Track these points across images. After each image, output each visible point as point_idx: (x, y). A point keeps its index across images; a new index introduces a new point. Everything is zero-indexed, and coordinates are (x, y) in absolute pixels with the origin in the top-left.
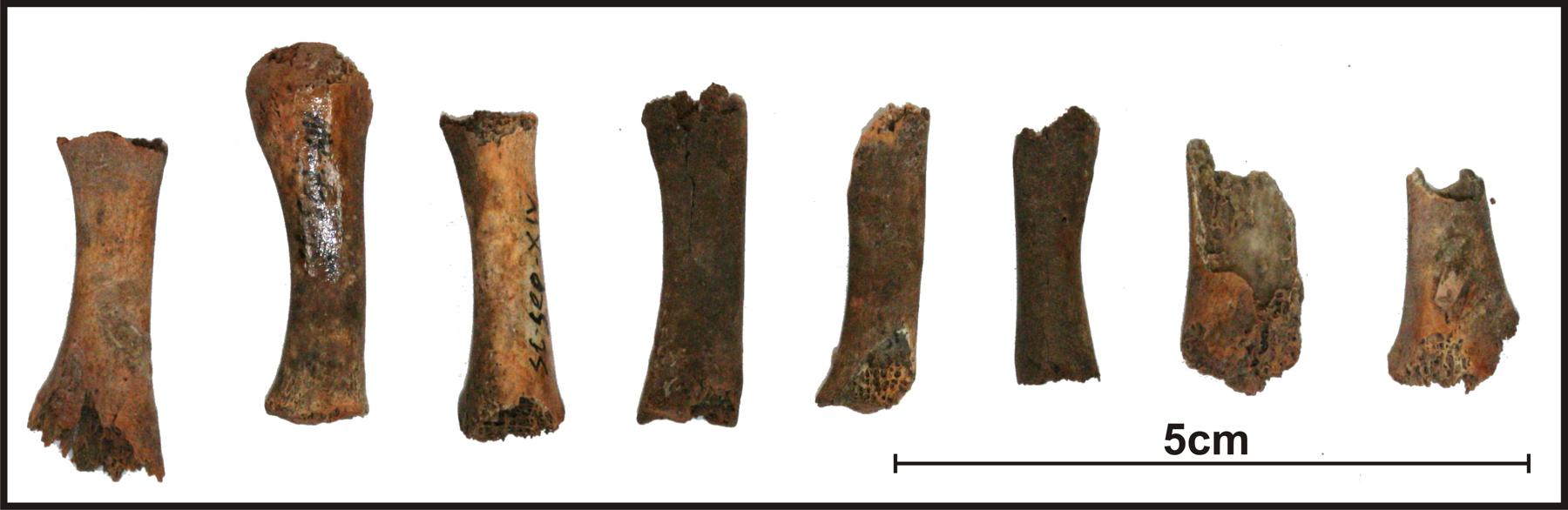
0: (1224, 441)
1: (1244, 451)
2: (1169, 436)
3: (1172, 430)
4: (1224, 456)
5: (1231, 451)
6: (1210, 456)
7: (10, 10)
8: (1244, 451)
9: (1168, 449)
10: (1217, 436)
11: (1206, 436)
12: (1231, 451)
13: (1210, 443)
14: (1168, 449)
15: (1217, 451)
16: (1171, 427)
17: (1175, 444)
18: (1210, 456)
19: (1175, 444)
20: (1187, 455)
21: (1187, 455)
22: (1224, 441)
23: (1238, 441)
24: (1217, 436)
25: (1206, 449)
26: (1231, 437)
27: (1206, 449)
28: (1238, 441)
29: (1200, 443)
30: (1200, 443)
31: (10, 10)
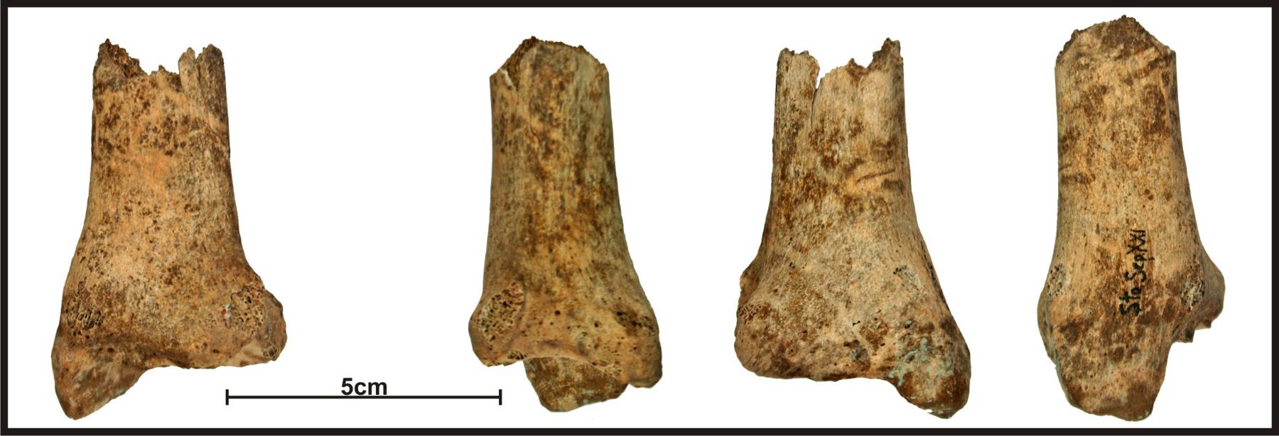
0: (374, 387)
1: (385, 392)
2: (344, 385)
3: (345, 382)
4: (374, 393)
5: (378, 392)
8: (385, 392)
10: (370, 385)
12: (378, 392)
13: (366, 388)
16: (345, 380)
17: (347, 389)
19: (347, 389)
20: (354, 393)
21: (354, 393)
22: (374, 387)
23: (381, 387)
24: (370, 385)
26: (378, 385)
28: (381, 387)
29: (361, 389)
30: (361, 389)
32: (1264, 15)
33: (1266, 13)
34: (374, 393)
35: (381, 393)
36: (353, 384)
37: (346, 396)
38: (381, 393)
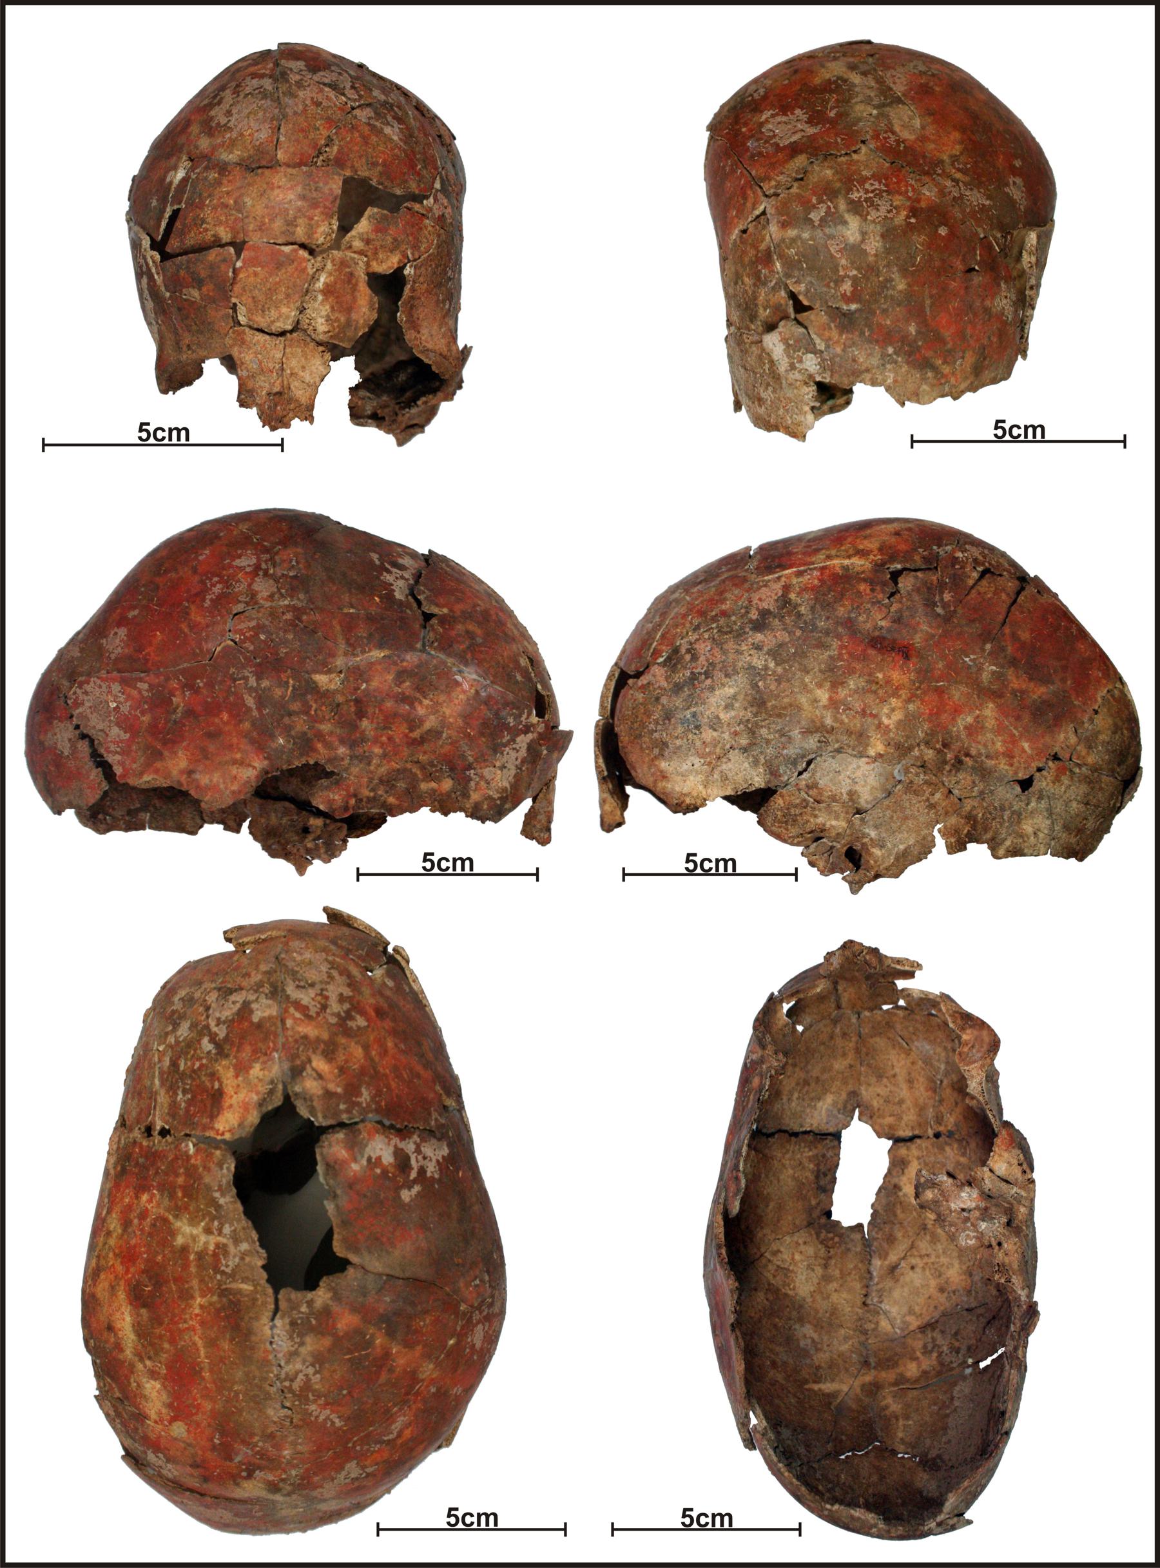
0: (175, 433)
1: (187, 439)
2: (141, 430)
4: (175, 441)
5: (179, 439)
6: (166, 441)
7: (8, 8)
8: (187, 439)
9: (140, 438)
10: (171, 430)
11: (163, 430)
12: (179, 439)
13: (166, 434)
14: (140, 438)
15: (170, 439)
17: (144, 435)
18: (166, 441)
20: (152, 441)
21: (152, 441)
22: (175, 433)
23: (183, 433)
24: (171, 430)
25: (164, 438)
26: (179, 431)
27: (164, 438)
28: (183, 433)
29: (160, 434)
30: (160, 434)
31: (8, 8)
32: (10, 10)
33: (10, 10)
34: (175, 441)
35: (183, 441)
36: (151, 429)
37: (143, 443)
38: (183, 441)
